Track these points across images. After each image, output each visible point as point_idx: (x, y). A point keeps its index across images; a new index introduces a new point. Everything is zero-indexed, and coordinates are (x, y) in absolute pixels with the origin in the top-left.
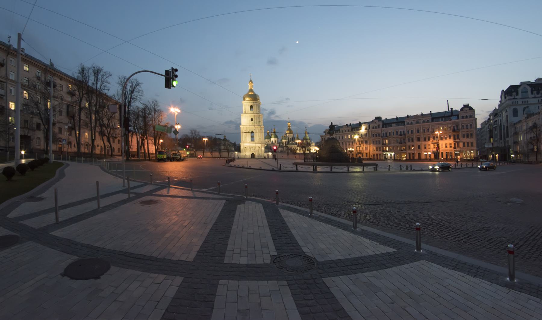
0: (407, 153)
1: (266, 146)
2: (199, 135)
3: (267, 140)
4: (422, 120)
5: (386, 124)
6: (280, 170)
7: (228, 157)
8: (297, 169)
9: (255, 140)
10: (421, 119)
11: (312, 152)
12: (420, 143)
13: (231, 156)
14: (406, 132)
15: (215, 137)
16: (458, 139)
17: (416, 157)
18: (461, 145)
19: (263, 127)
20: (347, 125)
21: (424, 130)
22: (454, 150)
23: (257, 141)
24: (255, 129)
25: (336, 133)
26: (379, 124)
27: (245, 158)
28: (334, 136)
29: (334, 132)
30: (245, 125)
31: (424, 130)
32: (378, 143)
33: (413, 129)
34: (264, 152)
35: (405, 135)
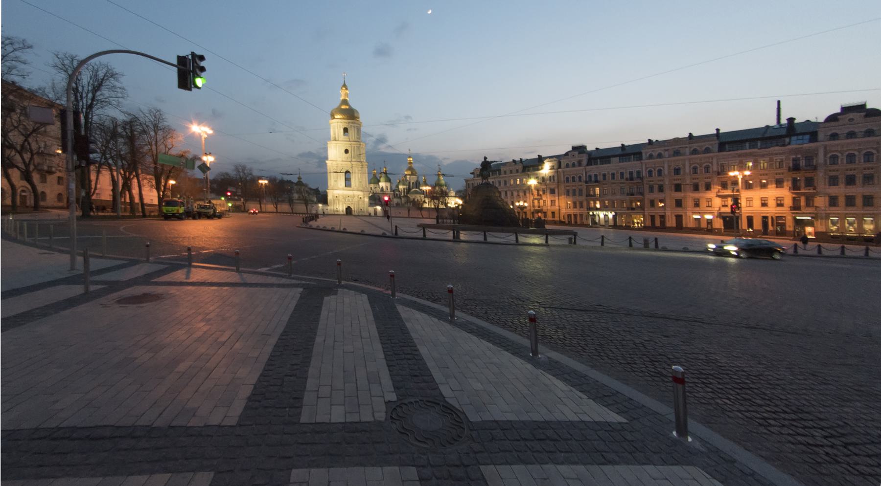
0: (646, 214)
1: (371, 194)
2: (251, 174)
3: (372, 186)
4: (690, 148)
5: (596, 159)
6: (396, 236)
7: (306, 212)
8: (424, 235)
9: (352, 186)
10: (686, 147)
11: (450, 207)
12: (683, 194)
13: (311, 210)
14: (644, 173)
15: (282, 178)
16: (812, 188)
17: (671, 222)
18: (820, 202)
19: (366, 163)
20: (514, 161)
21: (695, 169)
22: (793, 213)
23: (356, 186)
24: (352, 167)
25: (492, 175)
26: (581, 158)
27: (335, 215)
28: (491, 181)
29: (489, 174)
30: (335, 159)
31: (695, 169)
32: (577, 193)
33: (663, 167)
34: (368, 206)
35: (642, 179)
